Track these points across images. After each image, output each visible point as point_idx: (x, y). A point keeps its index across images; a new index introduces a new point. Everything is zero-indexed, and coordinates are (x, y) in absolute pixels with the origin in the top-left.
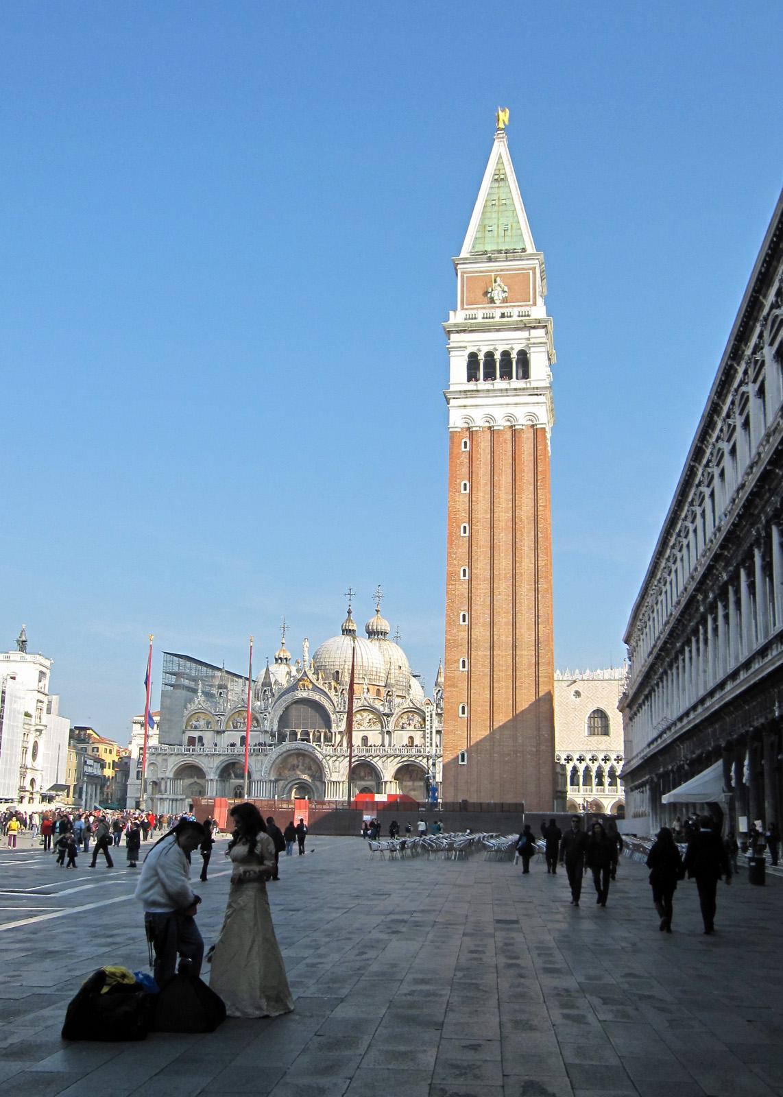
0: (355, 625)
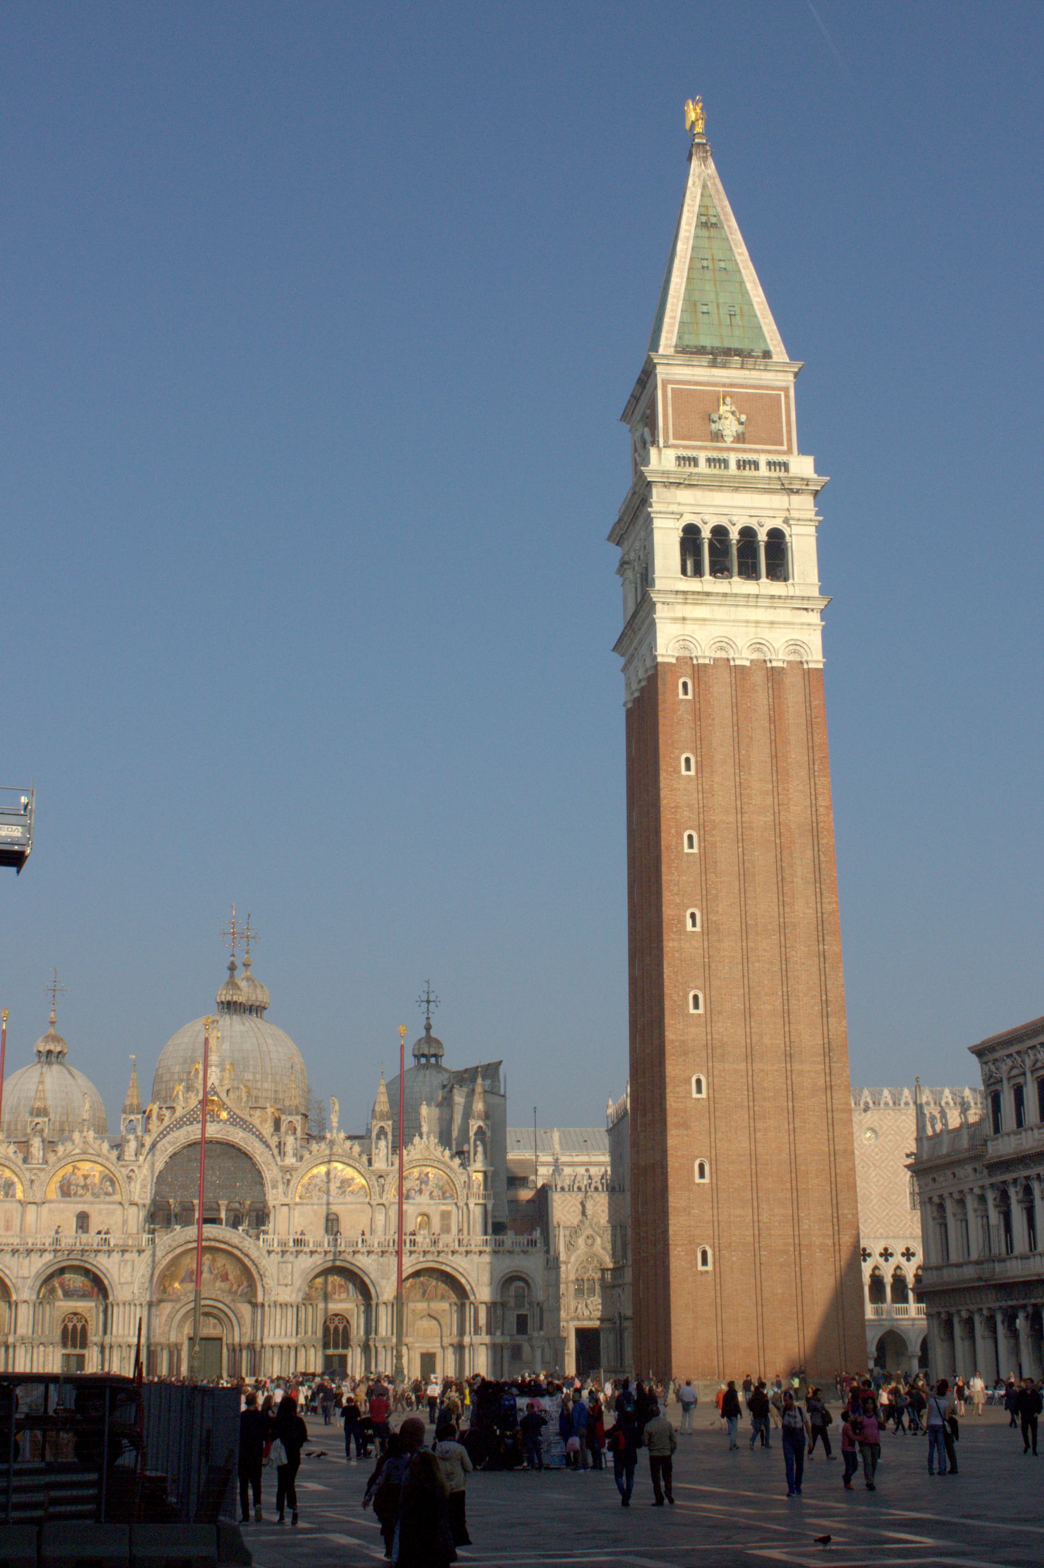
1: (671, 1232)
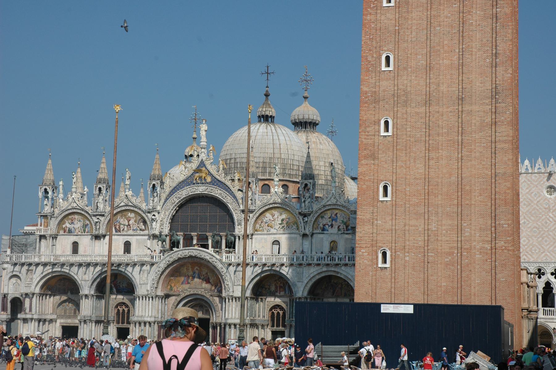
0: (273, 110)
1: (357, 238)
